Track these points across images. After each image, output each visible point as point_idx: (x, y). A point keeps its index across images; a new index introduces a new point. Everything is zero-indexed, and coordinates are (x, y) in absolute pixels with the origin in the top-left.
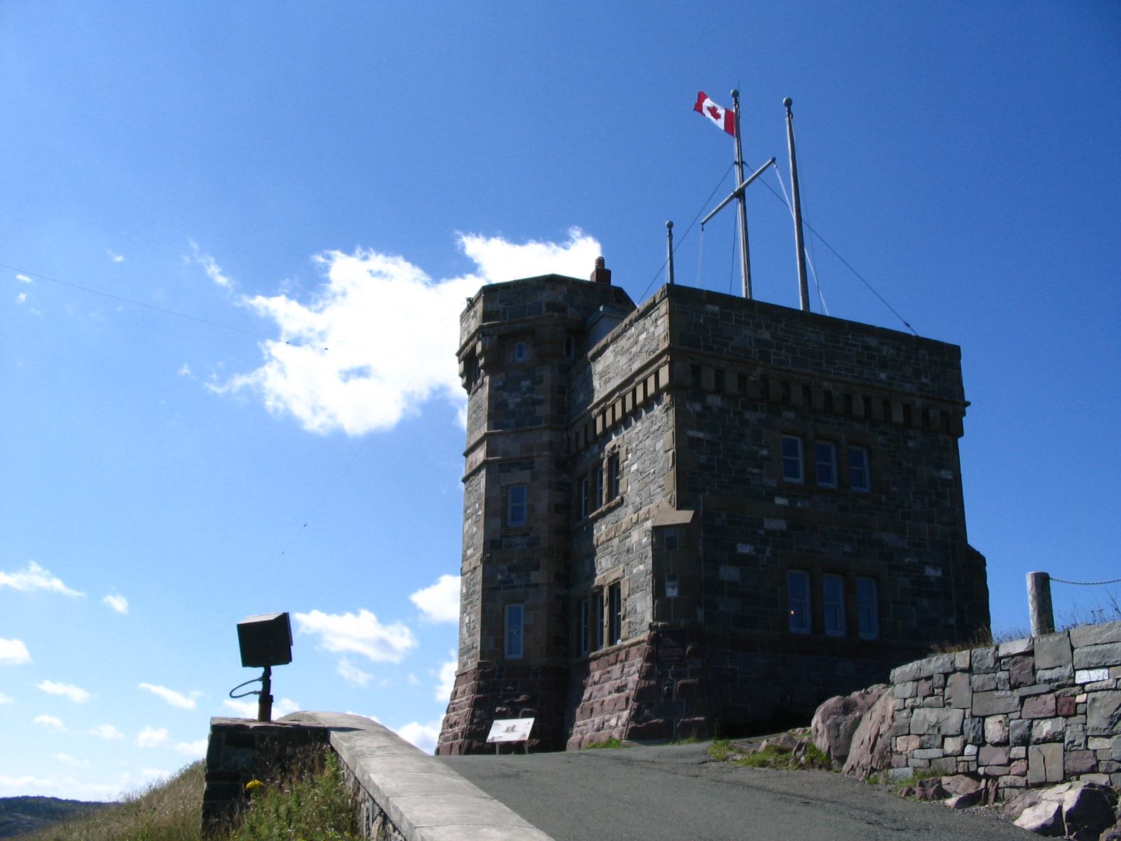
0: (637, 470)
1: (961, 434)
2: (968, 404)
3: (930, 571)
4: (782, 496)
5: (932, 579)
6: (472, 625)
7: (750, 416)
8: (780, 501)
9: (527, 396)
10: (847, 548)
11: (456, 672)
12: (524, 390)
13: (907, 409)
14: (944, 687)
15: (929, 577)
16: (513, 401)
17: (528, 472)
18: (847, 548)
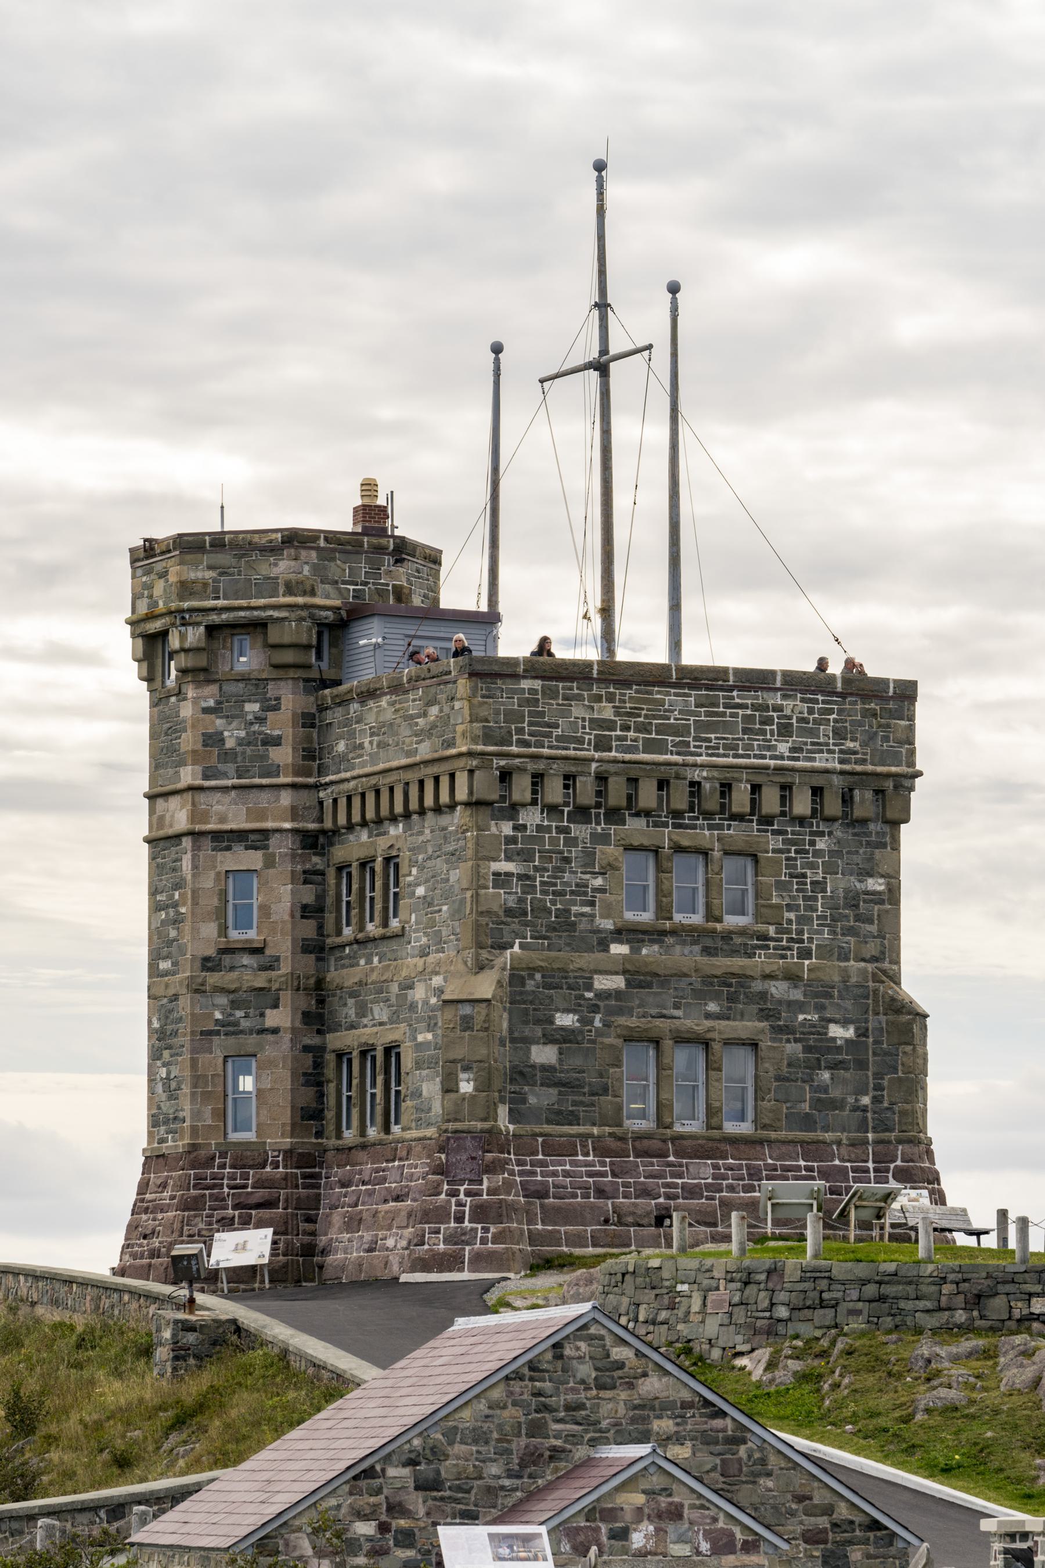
0: (425, 897)
1: (906, 820)
2: (919, 774)
3: (836, 1031)
4: (621, 942)
5: (839, 1042)
6: (173, 1085)
7: (580, 831)
8: (619, 949)
9: (256, 727)
10: (712, 1007)
11: (144, 1150)
12: (250, 717)
13: (817, 792)
14: (622, 1282)
15: (834, 1039)
16: (233, 735)
17: (259, 854)
18: (712, 1007)
